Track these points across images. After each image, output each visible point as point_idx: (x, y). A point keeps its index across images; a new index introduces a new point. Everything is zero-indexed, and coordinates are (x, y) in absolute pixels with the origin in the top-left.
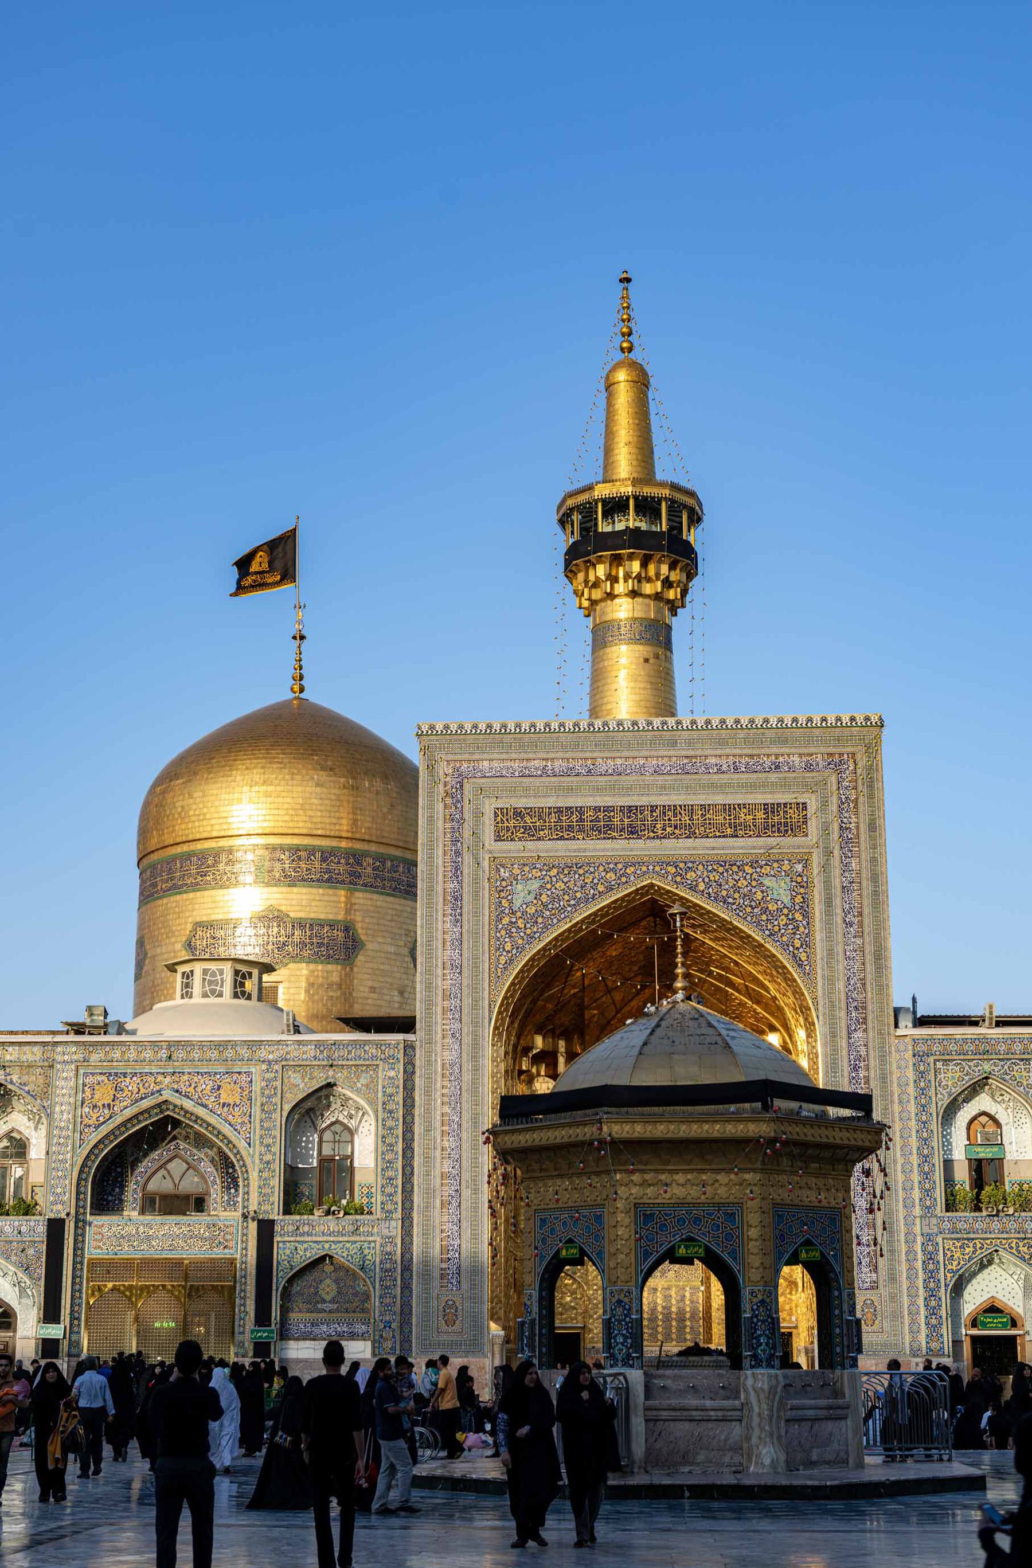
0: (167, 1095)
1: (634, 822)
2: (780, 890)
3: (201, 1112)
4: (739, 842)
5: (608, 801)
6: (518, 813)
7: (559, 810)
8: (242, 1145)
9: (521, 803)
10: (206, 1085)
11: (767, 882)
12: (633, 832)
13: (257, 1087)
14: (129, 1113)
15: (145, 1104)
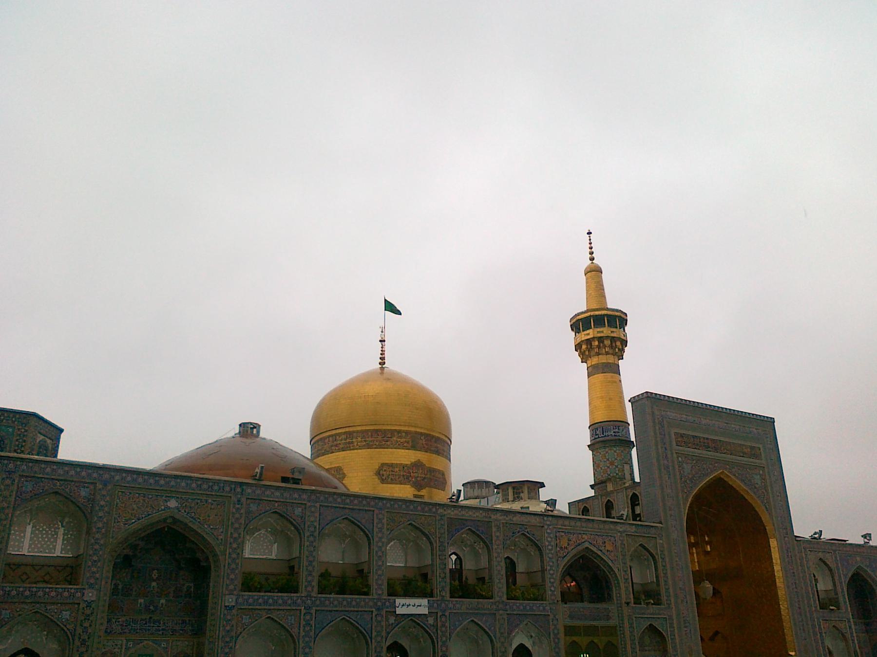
0: (587, 545)
1: (715, 446)
2: (757, 479)
3: (599, 553)
4: (745, 459)
5: (706, 436)
6: (682, 436)
7: (694, 437)
8: (616, 571)
9: (682, 432)
10: (600, 541)
11: (755, 476)
12: (716, 450)
13: (619, 543)
14: (574, 552)
15: (580, 548)
